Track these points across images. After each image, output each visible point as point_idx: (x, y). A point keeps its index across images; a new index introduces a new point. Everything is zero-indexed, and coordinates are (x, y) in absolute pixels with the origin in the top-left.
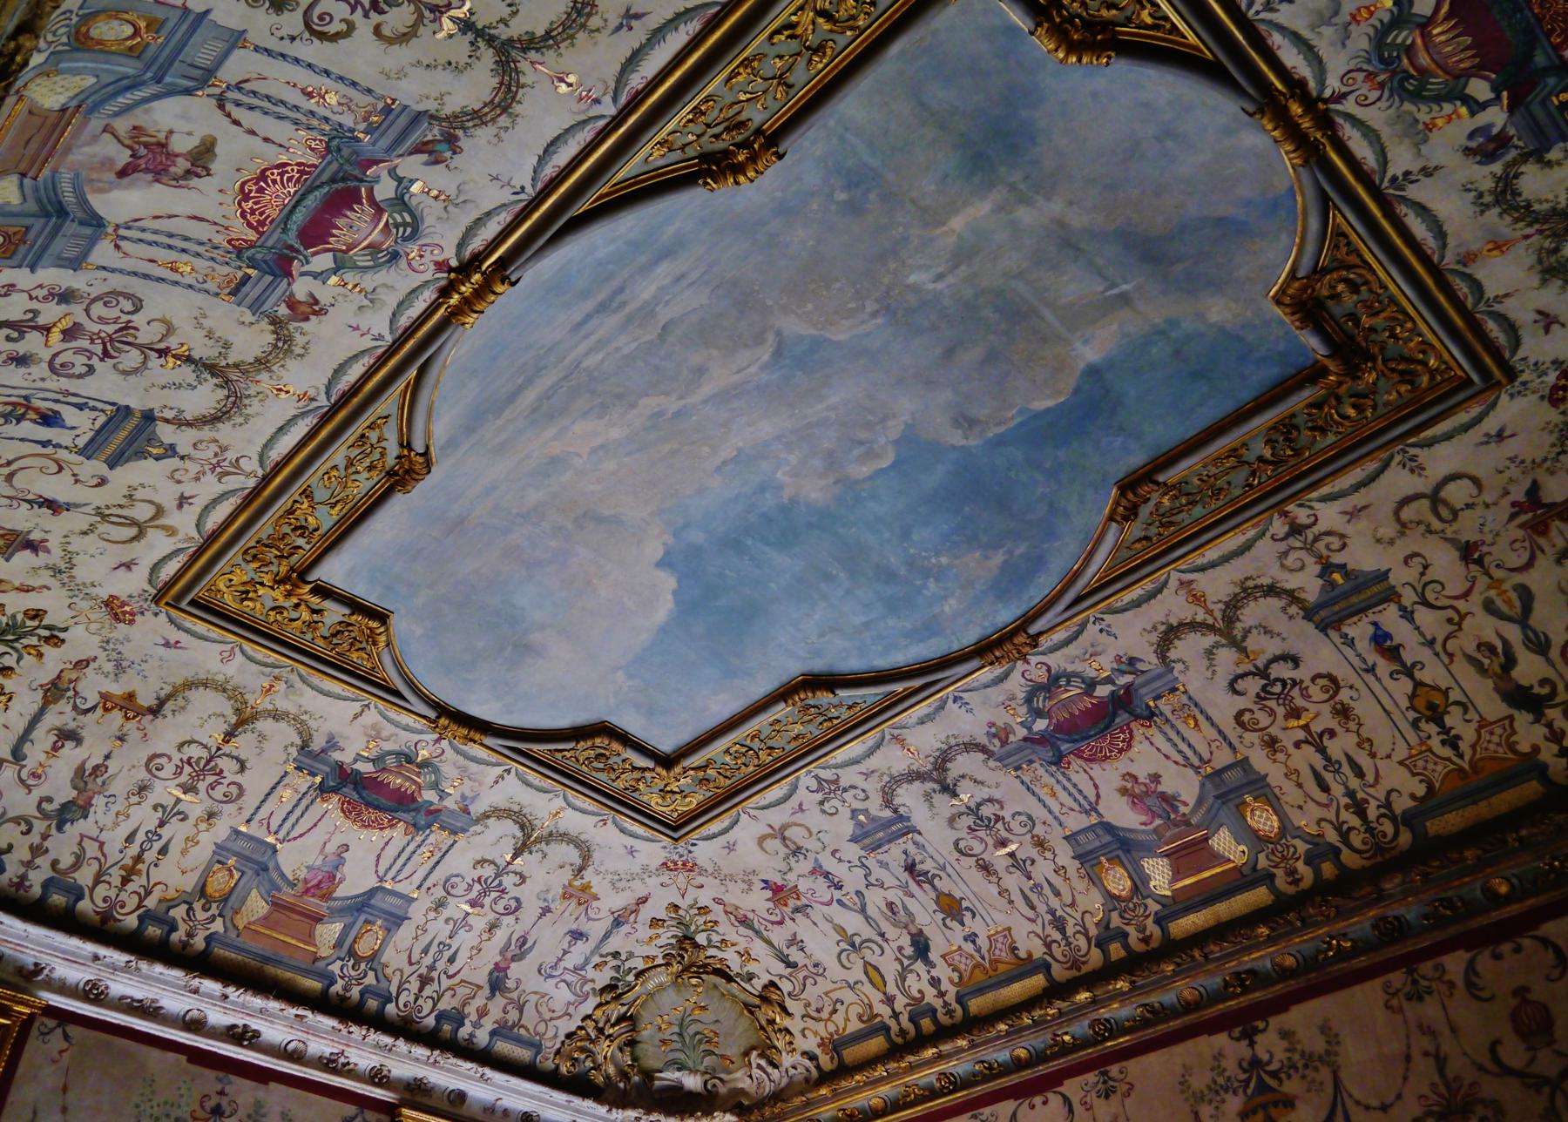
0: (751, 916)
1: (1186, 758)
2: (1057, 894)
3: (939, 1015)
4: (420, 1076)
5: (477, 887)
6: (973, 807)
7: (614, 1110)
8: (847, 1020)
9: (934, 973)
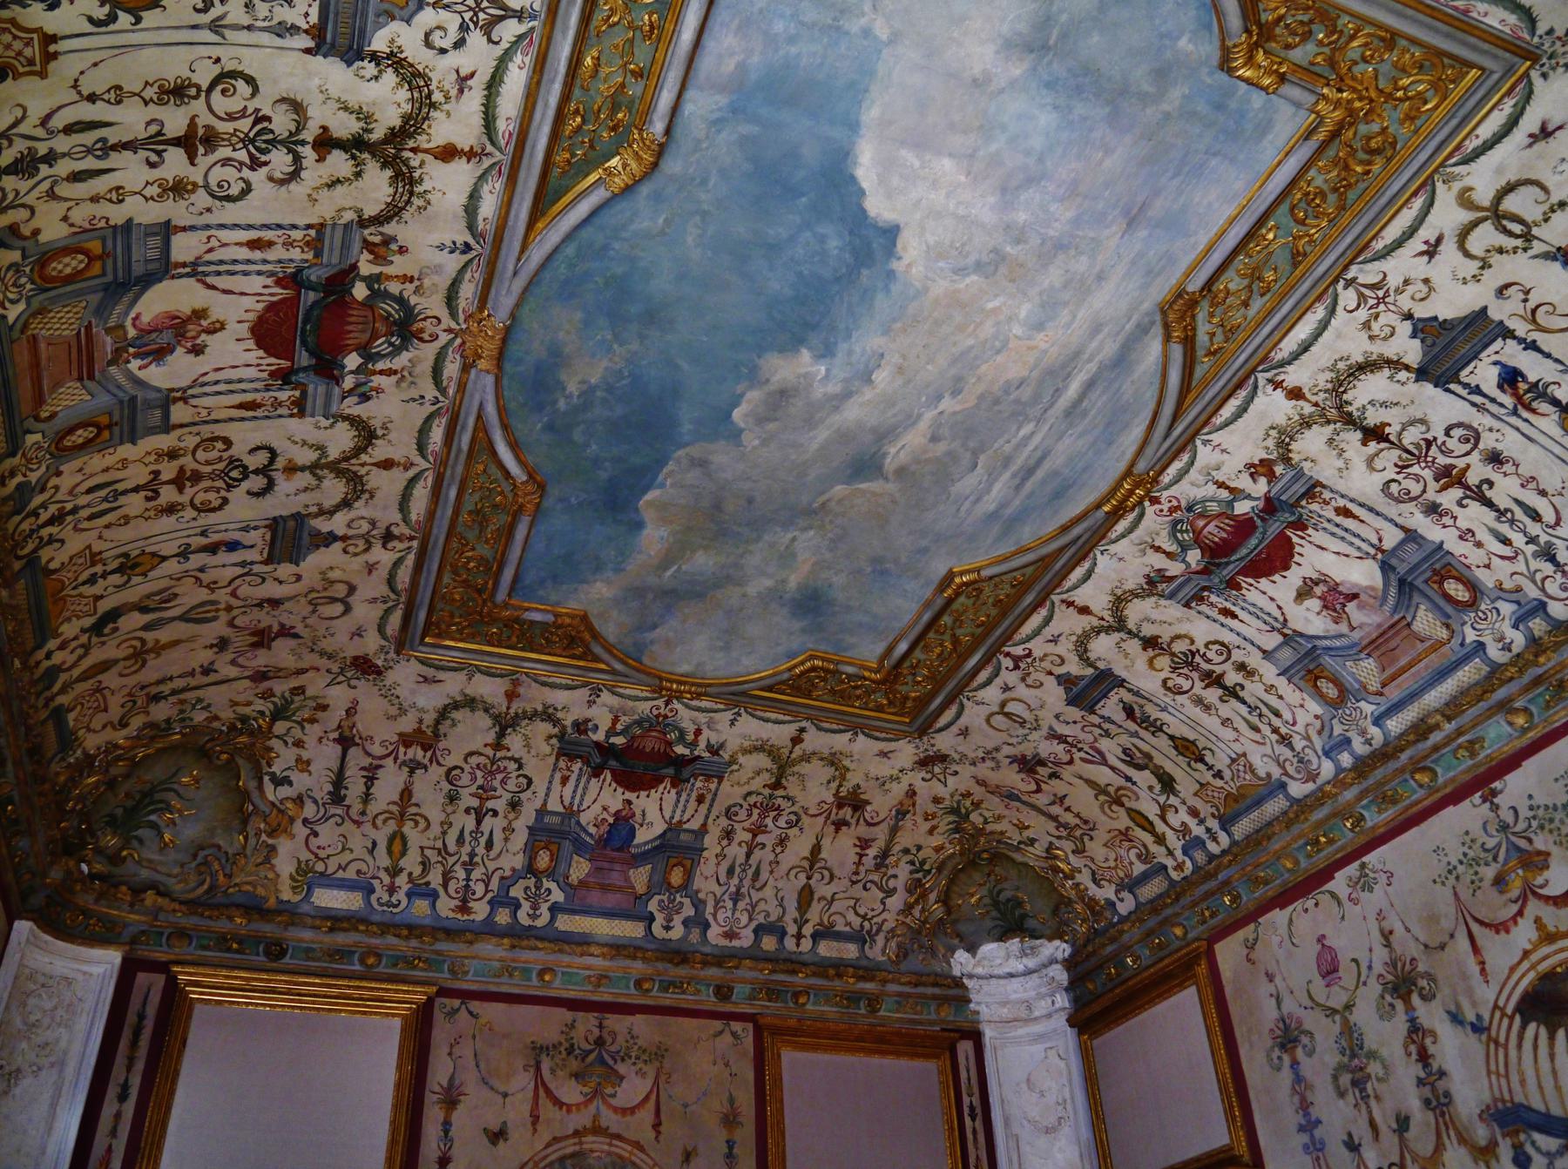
1: (204, 385)
2: (76, 177)
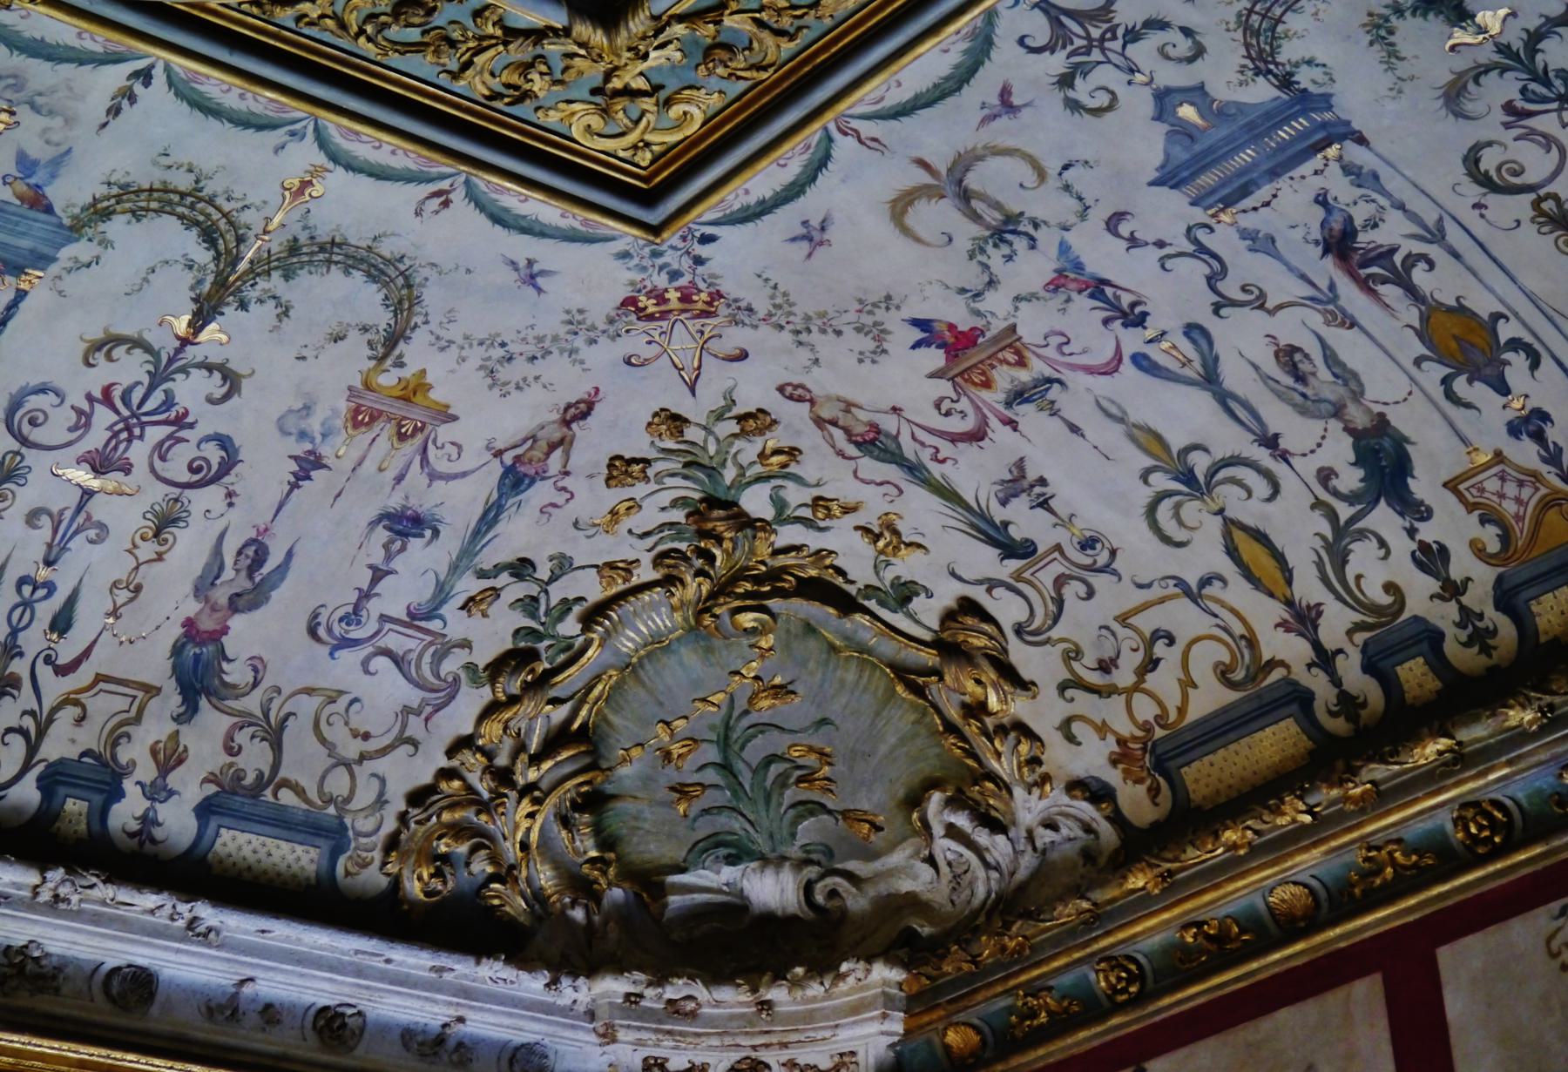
0: (889, 424)
3: (1451, 648)
4: (19, 941)
5: (103, 417)
6: (1517, 45)
7: (566, 982)
8: (1188, 683)
9: (1429, 532)
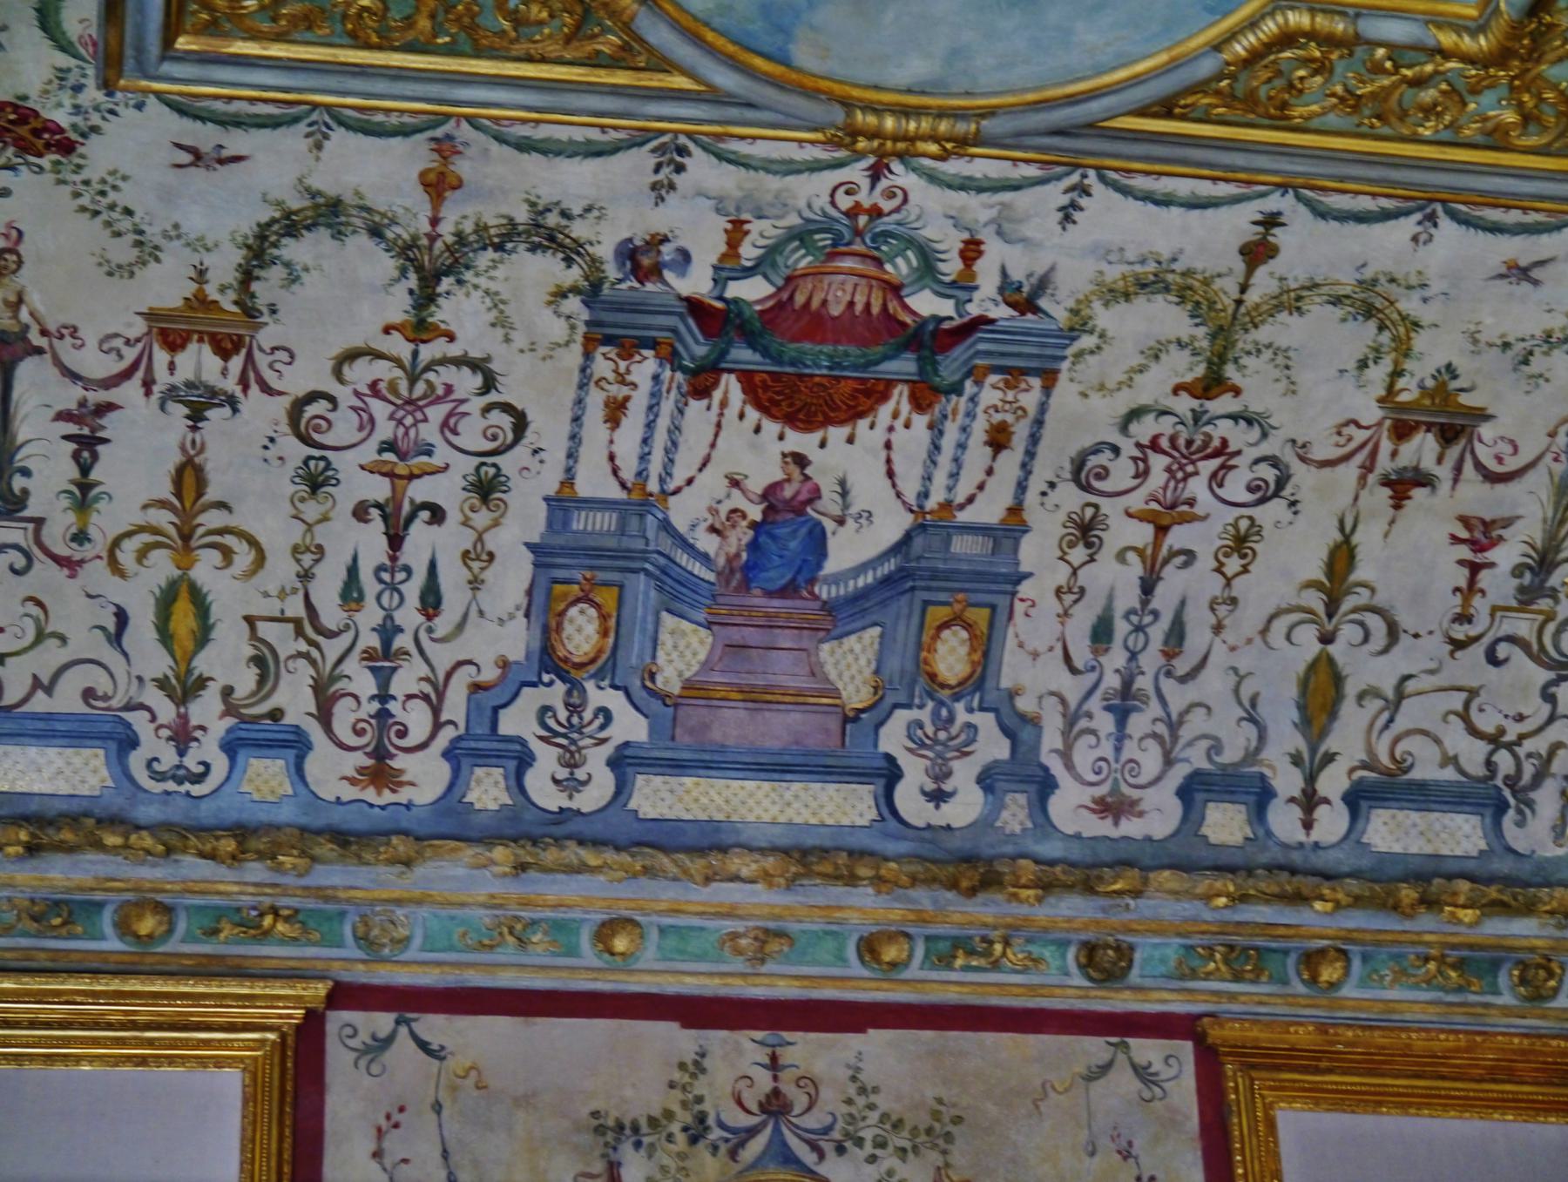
5: (1158, 462)
